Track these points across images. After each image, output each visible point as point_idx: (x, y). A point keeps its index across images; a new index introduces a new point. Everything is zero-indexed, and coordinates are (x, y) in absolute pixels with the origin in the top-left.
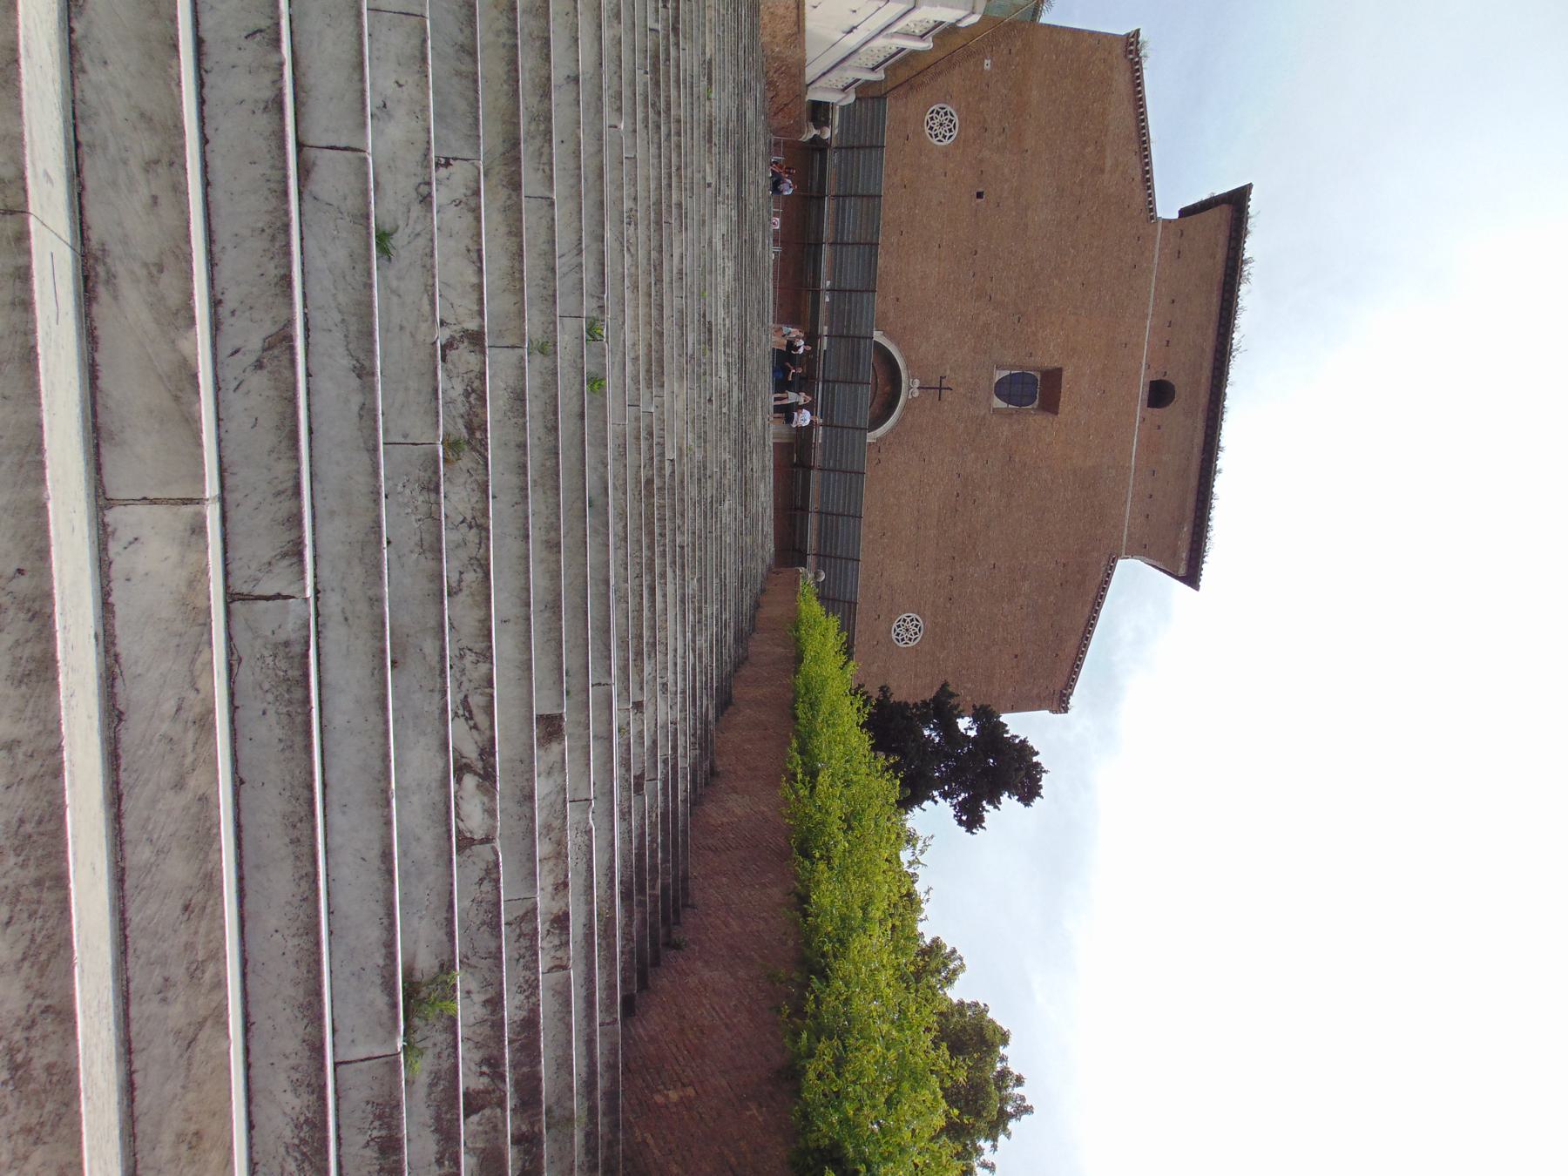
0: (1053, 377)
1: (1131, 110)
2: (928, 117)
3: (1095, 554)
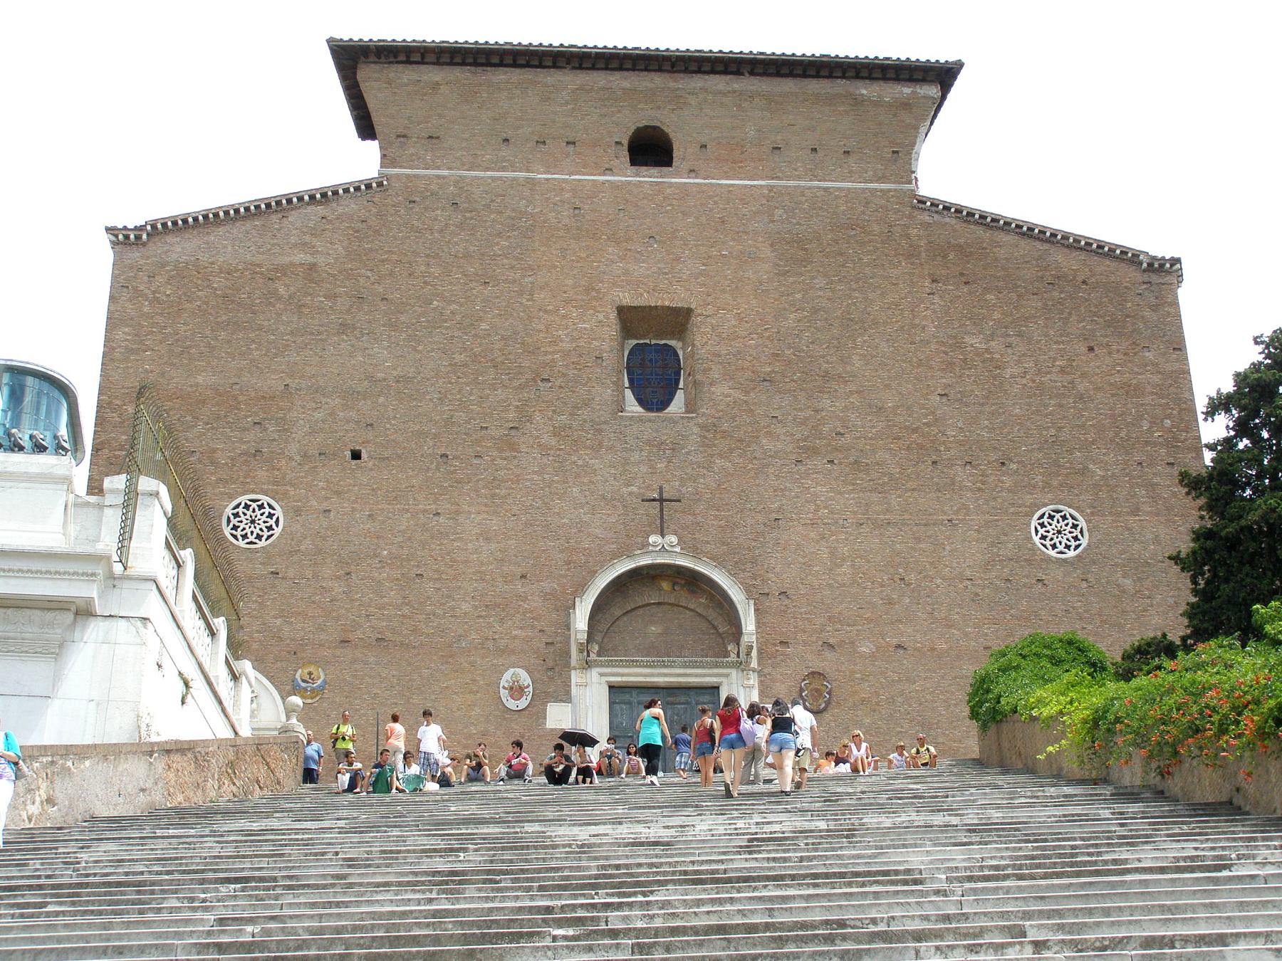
0: (630, 319)
1: (221, 230)
2: (242, 543)
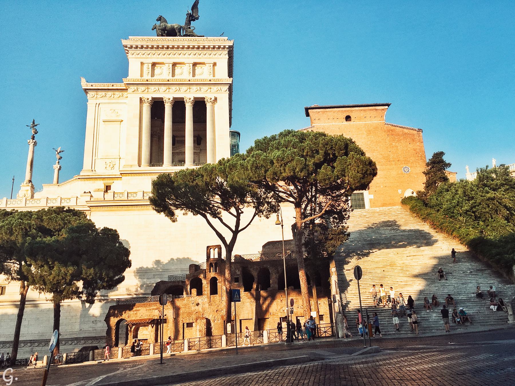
3: (385, 128)
